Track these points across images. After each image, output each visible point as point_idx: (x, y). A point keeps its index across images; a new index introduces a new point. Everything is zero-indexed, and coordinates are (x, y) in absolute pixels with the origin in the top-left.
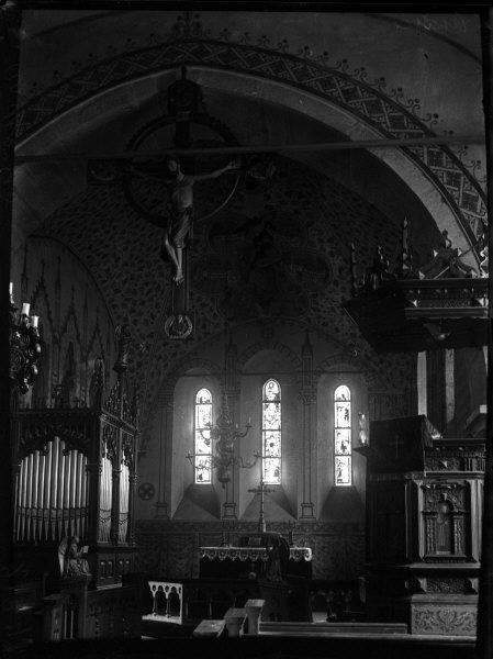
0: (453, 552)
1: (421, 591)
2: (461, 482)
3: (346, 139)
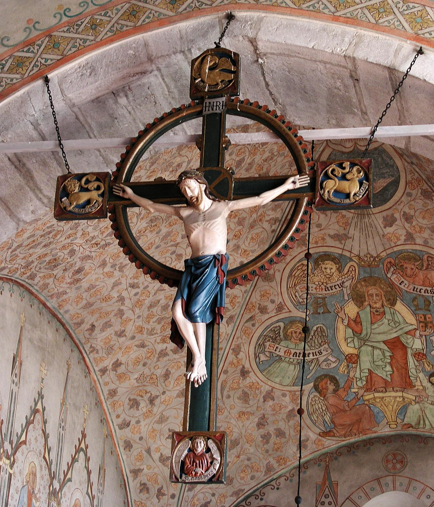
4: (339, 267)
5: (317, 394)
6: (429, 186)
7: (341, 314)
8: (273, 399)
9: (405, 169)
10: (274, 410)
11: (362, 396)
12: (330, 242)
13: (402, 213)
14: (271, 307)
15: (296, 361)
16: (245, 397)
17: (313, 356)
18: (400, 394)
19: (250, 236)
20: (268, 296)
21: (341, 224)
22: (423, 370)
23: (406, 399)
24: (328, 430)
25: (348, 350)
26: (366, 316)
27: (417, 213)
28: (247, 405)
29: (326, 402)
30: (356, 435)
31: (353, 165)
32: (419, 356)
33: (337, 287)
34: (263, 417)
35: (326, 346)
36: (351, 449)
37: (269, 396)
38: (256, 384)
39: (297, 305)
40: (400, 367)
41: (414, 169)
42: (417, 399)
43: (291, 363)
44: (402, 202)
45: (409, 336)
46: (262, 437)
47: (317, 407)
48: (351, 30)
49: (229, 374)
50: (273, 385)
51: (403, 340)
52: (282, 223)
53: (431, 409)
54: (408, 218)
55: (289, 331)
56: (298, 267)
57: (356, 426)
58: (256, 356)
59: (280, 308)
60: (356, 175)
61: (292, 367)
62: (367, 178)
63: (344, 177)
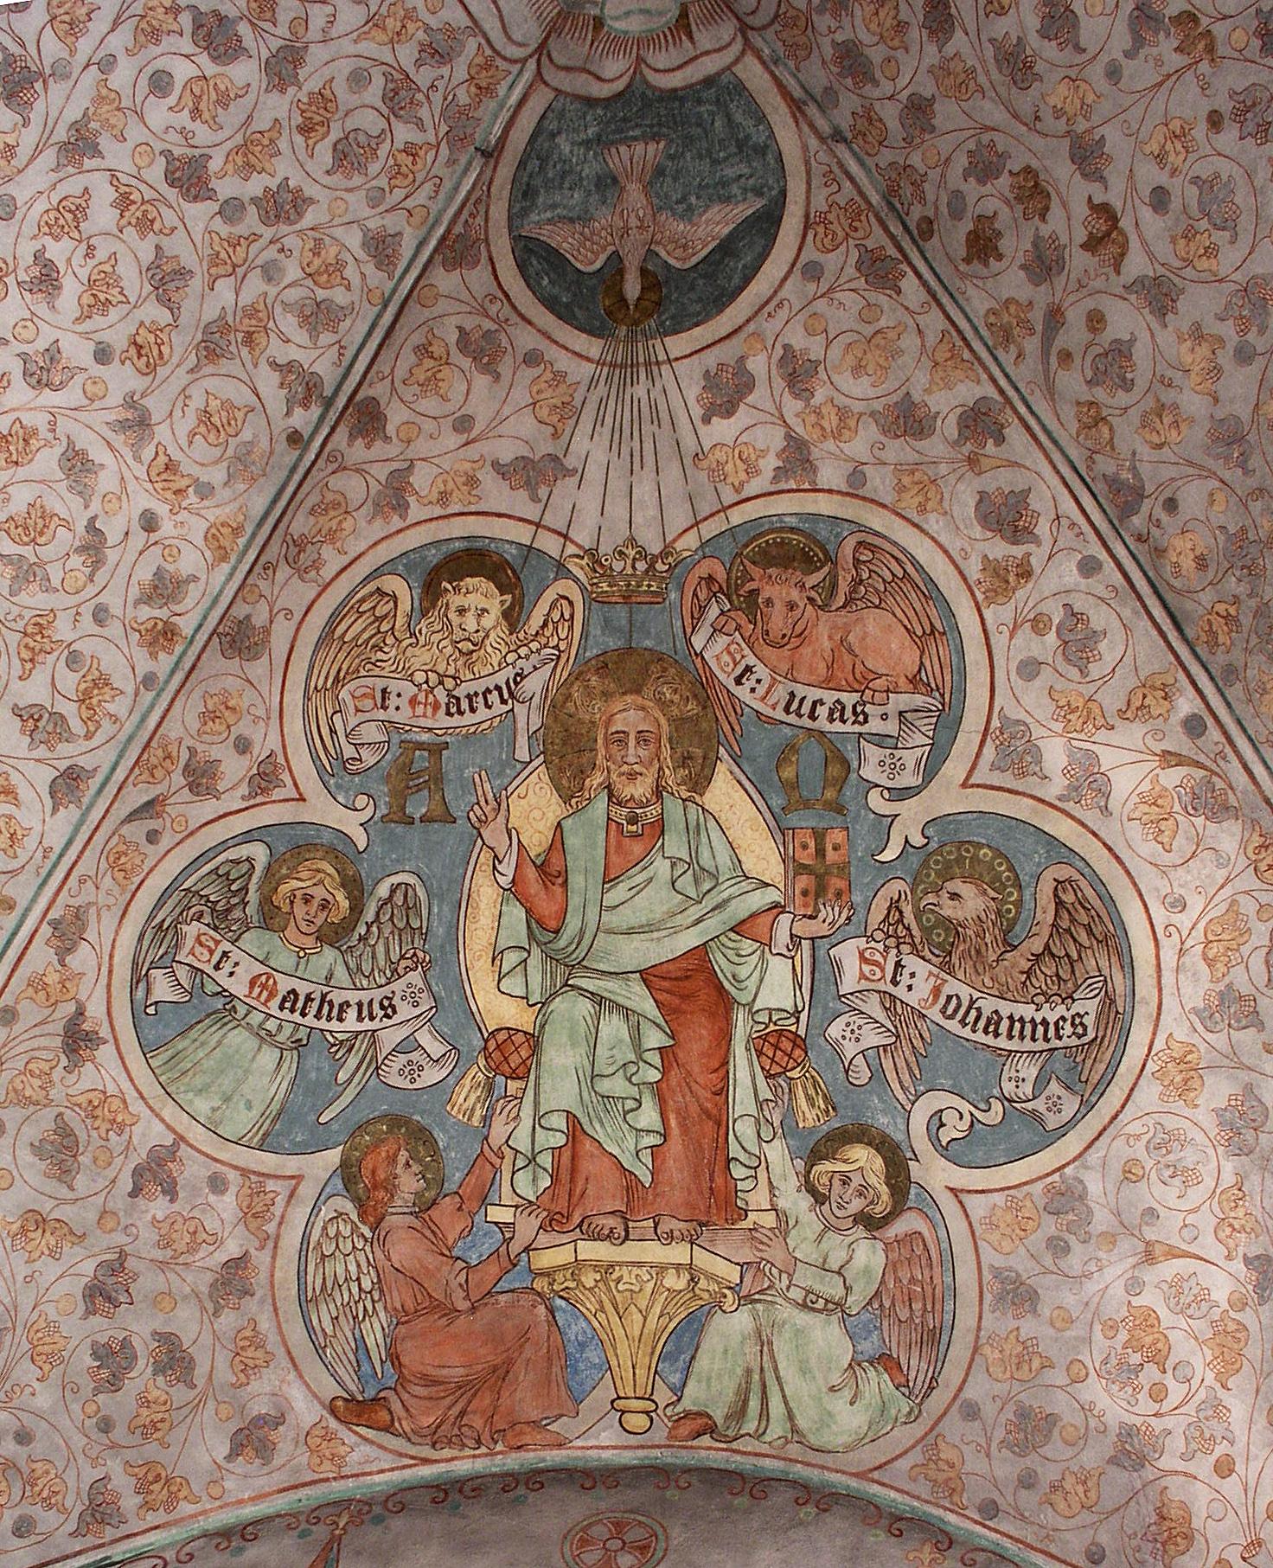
4: (512, 605)
5: (349, 1207)
6: (892, 237)
7: (494, 834)
8: (171, 1192)
9: (807, 163)
10: (165, 1243)
11: (527, 1249)
12: (495, 493)
13: (779, 351)
14: (234, 769)
15: (288, 1029)
16: (61, 1152)
17: (360, 1019)
18: (679, 1253)
19: (197, 402)
20: (231, 719)
21: (544, 413)
22: (789, 1129)
23: (703, 1283)
24: (370, 1393)
25: (501, 1009)
26: (586, 848)
27: (836, 351)
28: (64, 1192)
29: (379, 1254)
30: (479, 1442)
32: (783, 1047)
33: (494, 698)
34: (117, 1266)
35: (415, 977)
36: (447, 1495)
37: (157, 1174)
38: (116, 1104)
39: (337, 771)
40: (694, 1109)
41: (841, 165)
42: (748, 1279)
43: (265, 1037)
44: (780, 305)
45: (747, 946)
46: (95, 1355)
47: (340, 1271)
49: (18, 1028)
50: (182, 1123)
51: (720, 962)
52: (332, 416)
53: (799, 1332)
54: (798, 373)
55: (284, 889)
56: (362, 601)
57: (486, 1400)
58: (139, 977)
59: (265, 779)
61: (269, 1057)
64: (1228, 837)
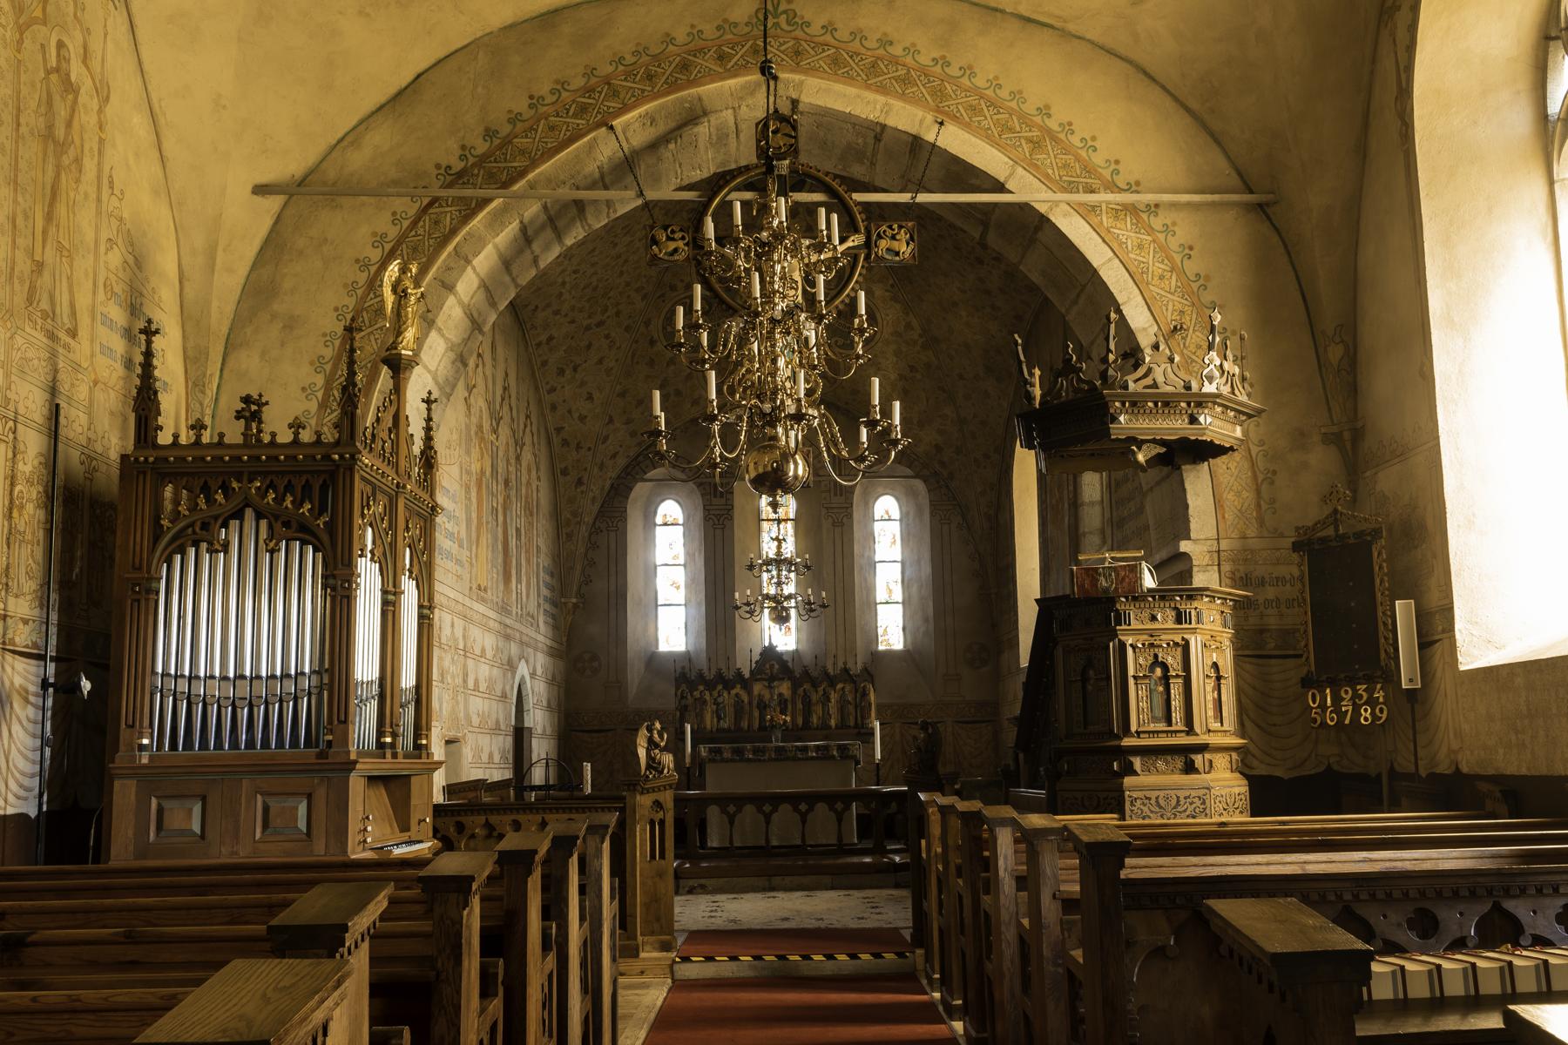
0: (1169, 723)
1: (1135, 773)
2: (1178, 639)
3: (1000, 188)
16: (651, 363)
31: (900, 227)
48: (881, 99)
58: (664, 328)
60: (903, 236)
62: (912, 238)
63: (893, 238)
64: (898, 306)
